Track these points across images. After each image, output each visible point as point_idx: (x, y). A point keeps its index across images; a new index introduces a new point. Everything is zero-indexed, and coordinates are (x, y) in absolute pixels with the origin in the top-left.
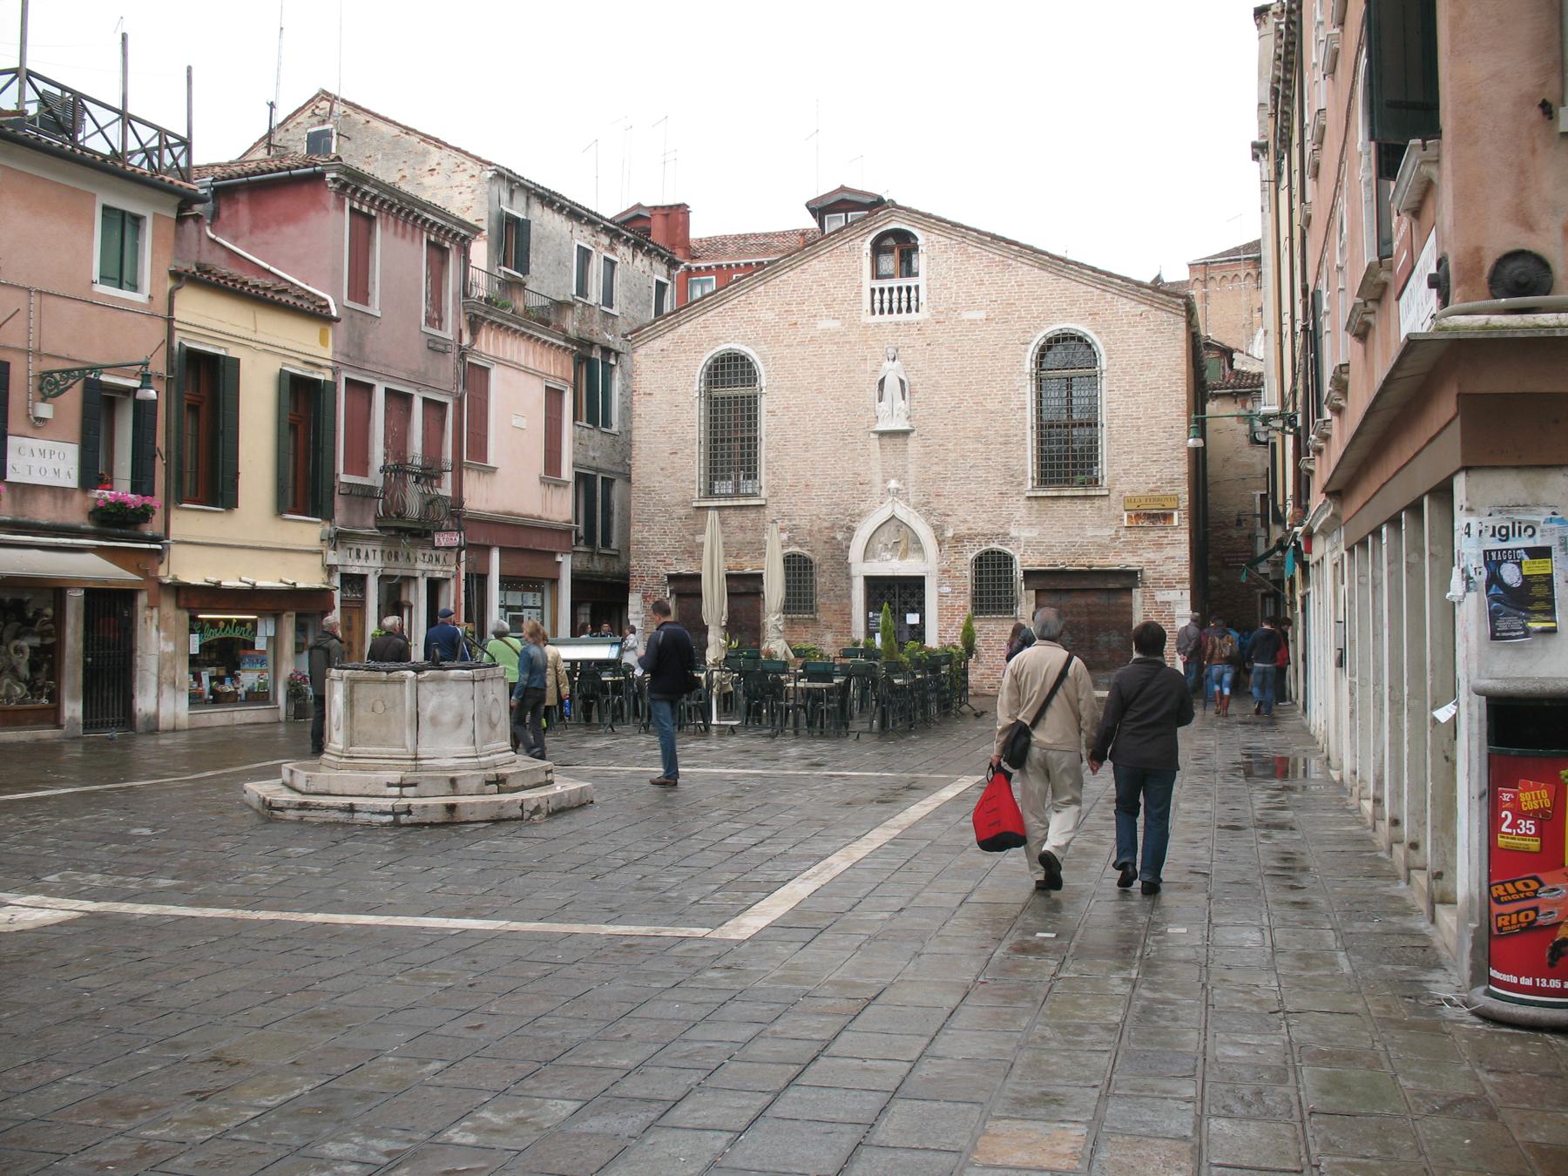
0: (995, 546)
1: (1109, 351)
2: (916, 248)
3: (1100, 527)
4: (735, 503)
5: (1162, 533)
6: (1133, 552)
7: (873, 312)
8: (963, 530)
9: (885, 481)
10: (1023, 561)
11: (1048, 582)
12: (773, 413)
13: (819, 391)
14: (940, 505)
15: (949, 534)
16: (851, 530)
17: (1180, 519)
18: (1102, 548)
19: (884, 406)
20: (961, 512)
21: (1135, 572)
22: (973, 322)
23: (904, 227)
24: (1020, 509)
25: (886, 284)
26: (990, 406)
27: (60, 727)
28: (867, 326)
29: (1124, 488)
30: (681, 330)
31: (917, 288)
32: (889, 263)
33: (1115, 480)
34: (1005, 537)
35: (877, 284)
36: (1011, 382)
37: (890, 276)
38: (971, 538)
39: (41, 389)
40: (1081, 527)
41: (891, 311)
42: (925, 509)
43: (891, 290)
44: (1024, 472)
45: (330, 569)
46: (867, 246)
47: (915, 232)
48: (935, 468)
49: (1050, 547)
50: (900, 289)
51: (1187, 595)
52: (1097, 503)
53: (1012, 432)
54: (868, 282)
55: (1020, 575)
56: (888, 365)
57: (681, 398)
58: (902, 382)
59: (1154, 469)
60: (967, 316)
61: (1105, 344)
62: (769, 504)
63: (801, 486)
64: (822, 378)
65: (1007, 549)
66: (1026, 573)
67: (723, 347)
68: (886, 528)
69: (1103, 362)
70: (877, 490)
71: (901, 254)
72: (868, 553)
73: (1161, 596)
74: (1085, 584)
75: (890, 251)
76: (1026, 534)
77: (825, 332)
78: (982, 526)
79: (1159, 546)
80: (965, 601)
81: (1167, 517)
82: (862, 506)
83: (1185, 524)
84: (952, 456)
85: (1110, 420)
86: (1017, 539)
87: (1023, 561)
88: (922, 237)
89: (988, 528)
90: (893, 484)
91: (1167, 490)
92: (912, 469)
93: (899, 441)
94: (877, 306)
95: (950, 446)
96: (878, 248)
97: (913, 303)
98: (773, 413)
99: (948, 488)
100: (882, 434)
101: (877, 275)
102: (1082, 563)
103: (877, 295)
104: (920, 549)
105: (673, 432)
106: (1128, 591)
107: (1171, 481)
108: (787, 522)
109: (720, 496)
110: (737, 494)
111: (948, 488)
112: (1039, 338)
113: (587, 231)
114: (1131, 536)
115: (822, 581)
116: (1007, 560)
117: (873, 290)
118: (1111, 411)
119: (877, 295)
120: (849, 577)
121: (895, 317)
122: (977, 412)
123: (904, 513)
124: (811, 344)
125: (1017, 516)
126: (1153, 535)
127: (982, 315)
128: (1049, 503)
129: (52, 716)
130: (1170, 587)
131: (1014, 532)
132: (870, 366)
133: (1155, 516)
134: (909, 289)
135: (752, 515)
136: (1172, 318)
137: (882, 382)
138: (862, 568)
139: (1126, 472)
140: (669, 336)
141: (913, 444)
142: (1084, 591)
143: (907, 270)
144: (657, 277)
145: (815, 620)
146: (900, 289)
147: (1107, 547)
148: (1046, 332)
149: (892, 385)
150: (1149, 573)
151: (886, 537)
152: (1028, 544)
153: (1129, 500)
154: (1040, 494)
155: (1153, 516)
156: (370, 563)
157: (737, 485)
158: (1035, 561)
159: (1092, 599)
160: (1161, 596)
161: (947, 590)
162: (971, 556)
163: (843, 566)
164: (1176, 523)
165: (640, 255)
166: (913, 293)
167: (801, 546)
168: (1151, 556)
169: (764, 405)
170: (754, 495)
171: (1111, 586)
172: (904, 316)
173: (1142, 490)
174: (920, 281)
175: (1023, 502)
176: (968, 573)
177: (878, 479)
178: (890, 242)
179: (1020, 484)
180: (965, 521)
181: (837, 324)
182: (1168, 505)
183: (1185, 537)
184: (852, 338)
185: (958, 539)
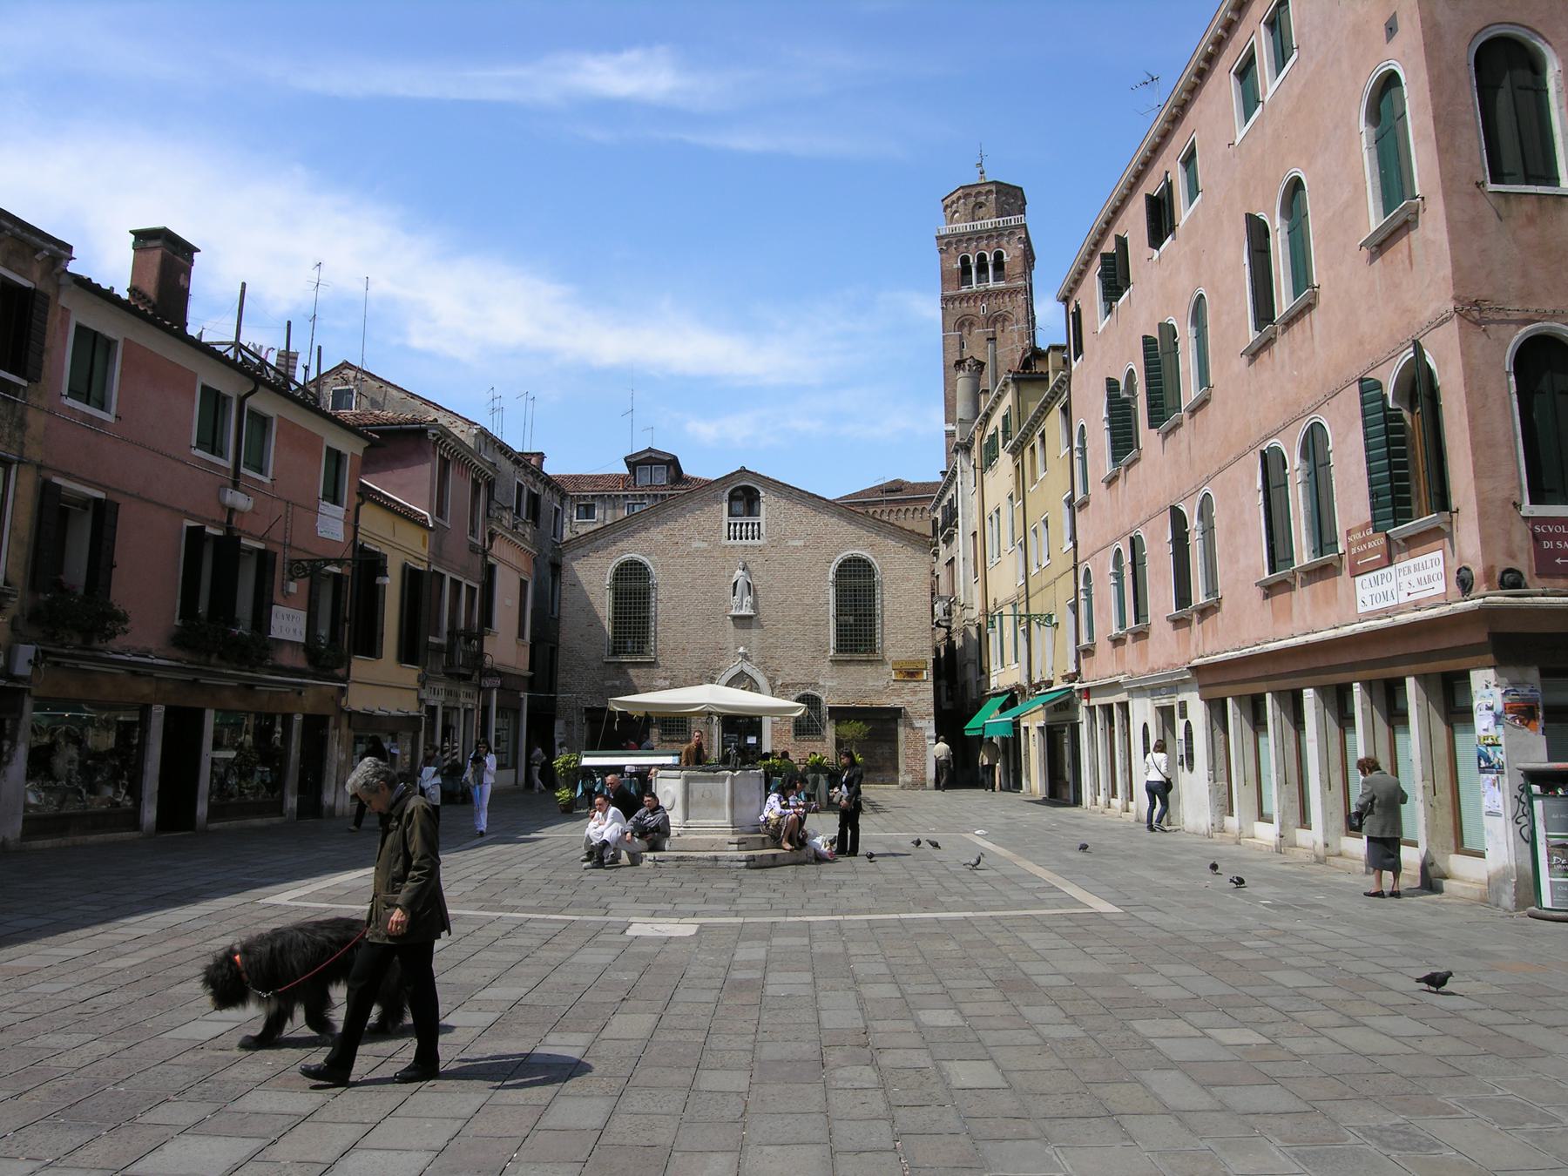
0: (809, 691)
8: (788, 680)
10: (828, 700)
14: (774, 664)
17: (927, 675)
22: (796, 547)
24: (826, 667)
25: (738, 520)
27: (282, 815)
34: (816, 685)
38: (794, 685)
39: (290, 571)
42: (763, 666)
45: (421, 701)
46: (726, 496)
51: (933, 723)
67: (627, 557)
75: (739, 499)
78: (800, 678)
83: (931, 678)
87: (828, 700)
88: (762, 494)
89: (805, 679)
90: (741, 650)
91: (920, 657)
111: (779, 652)
112: (838, 559)
114: (897, 685)
123: (748, 668)
124: (687, 561)
126: (911, 685)
127: (801, 543)
129: (278, 808)
152: (831, 689)
153: (895, 663)
155: (912, 674)
156: (437, 701)
173: (904, 657)
174: (762, 519)
177: (732, 646)
178: (740, 493)
181: (705, 545)
183: (930, 686)
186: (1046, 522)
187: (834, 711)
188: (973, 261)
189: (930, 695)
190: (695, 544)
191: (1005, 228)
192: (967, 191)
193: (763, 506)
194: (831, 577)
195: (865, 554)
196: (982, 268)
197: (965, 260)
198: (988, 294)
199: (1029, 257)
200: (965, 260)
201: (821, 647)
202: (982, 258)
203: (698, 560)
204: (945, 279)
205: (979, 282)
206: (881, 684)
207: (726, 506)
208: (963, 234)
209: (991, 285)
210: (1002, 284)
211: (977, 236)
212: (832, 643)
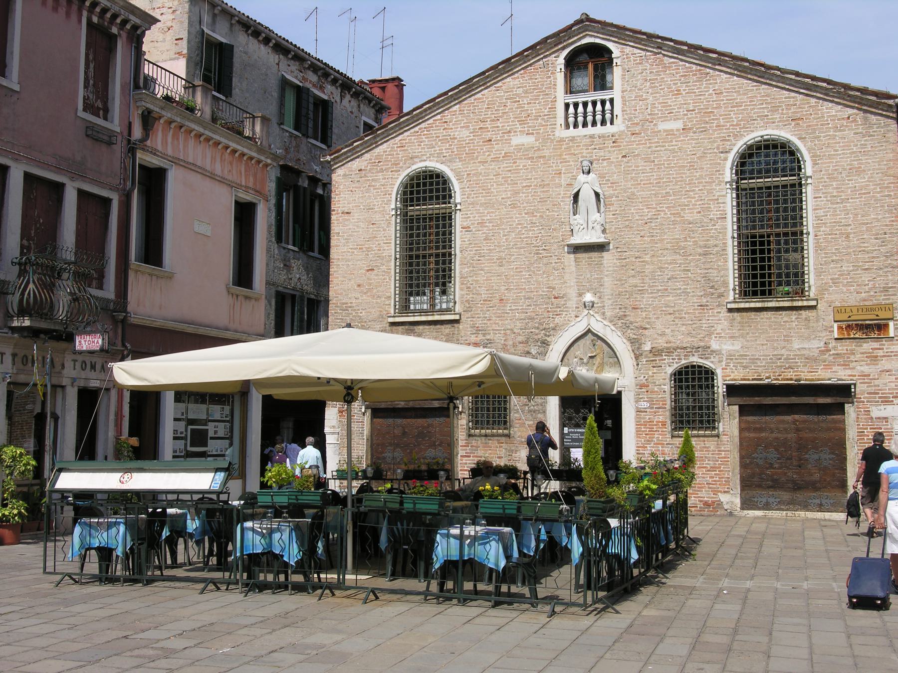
0: (695, 360)
1: (814, 157)
2: (611, 60)
3: (808, 339)
4: (430, 318)
5: (876, 345)
6: (845, 365)
7: (567, 126)
8: (661, 343)
9: (580, 295)
11: (754, 398)
12: (466, 228)
13: (514, 206)
15: (647, 347)
16: (545, 344)
19: (579, 219)
20: (659, 325)
21: (848, 387)
22: (669, 132)
23: (598, 41)
24: (722, 321)
25: (580, 98)
26: (688, 217)
28: (562, 140)
29: (833, 297)
30: (377, 150)
31: (612, 101)
32: (584, 80)
33: (822, 290)
34: (705, 350)
35: (571, 99)
36: (710, 192)
38: (669, 351)
40: (788, 339)
41: (585, 125)
42: (622, 321)
43: (585, 104)
44: (725, 284)
47: (610, 45)
48: (633, 281)
49: (754, 360)
50: (594, 103)
52: (804, 314)
53: (711, 242)
54: (561, 97)
55: (720, 389)
56: (582, 178)
57: (377, 217)
58: (597, 195)
59: (866, 278)
60: (663, 126)
61: (809, 150)
62: (463, 319)
63: (496, 301)
64: (516, 193)
65: (708, 363)
67: (419, 166)
69: (808, 169)
70: (572, 303)
71: (596, 69)
76: (727, 347)
77: (519, 148)
78: (681, 339)
80: (665, 416)
84: (649, 268)
85: (817, 227)
89: (687, 341)
90: (588, 297)
91: (882, 299)
92: (608, 282)
94: (571, 120)
95: (647, 258)
96: (573, 64)
97: (608, 116)
98: (466, 228)
99: (645, 300)
100: (578, 249)
101: (570, 90)
102: (788, 377)
103: (571, 109)
104: (618, 363)
105: (369, 249)
106: (840, 409)
108: (481, 337)
109: (415, 312)
110: (432, 310)
111: (645, 300)
112: (739, 146)
113: (295, 66)
114: (842, 348)
116: (708, 375)
117: (567, 106)
118: (818, 218)
119: (571, 109)
121: (590, 130)
122: (674, 223)
123: (598, 327)
125: (719, 328)
126: (868, 346)
127: (678, 125)
128: (752, 315)
131: (715, 346)
133: (868, 327)
134: (603, 103)
136: (882, 120)
137: (576, 196)
139: (835, 282)
140: (367, 156)
142: (791, 409)
143: (601, 83)
144: (364, 118)
145: (508, 436)
147: (815, 360)
148: (745, 139)
149: (587, 196)
150: (861, 389)
152: (730, 356)
153: (838, 310)
154: (742, 305)
158: (739, 376)
161: (644, 405)
162: (670, 370)
164: (892, 334)
165: (348, 97)
168: (866, 369)
169: (459, 220)
170: (448, 310)
172: (599, 129)
173: (853, 300)
174: (616, 93)
175: (724, 314)
176: (667, 388)
177: (573, 293)
178: (584, 57)
179: (721, 295)
180: (663, 334)
181: (531, 139)
184: (546, 153)
187: (733, 390)
190: (518, 140)
194: (728, 174)
201: (713, 289)
203: (521, 163)
206: (816, 345)
207: (560, 78)
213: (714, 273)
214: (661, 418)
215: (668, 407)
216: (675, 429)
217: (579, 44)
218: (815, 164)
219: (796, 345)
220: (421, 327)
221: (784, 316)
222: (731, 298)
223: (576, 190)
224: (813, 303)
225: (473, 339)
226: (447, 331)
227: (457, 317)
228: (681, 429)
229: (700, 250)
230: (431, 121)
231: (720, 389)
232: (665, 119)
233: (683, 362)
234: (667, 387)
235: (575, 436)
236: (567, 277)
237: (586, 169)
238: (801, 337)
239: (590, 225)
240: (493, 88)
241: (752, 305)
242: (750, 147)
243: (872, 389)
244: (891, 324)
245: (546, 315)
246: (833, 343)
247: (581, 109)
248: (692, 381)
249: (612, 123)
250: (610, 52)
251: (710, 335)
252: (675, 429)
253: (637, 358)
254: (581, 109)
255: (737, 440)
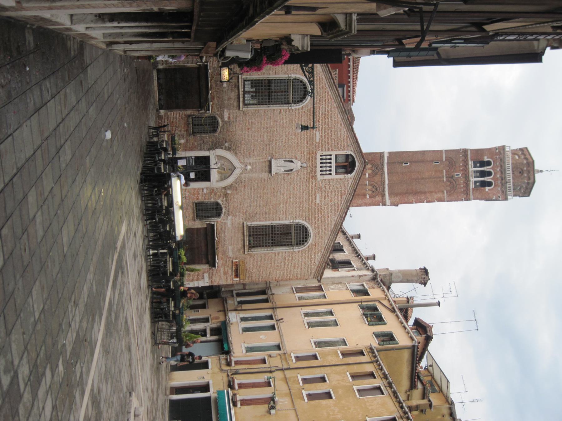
0: (224, 210)
3: (232, 251)
5: (230, 274)
7: (321, 156)
9: (250, 164)
15: (229, 192)
16: (229, 149)
18: (225, 253)
21: (214, 266)
24: (239, 219)
25: (333, 161)
28: (316, 154)
31: (331, 174)
32: (341, 160)
34: (227, 214)
35: (333, 157)
37: (336, 162)
38: (227, 200)
43: (330, 163)
44: (254, 221)
46: (349, 152)
47: (354, 173)
49: (224, 232)
51: (207, 285)
52: (242, 250)
54: (334, 153)
56: (299, 163)
58: (292, 170)
62: (240, 112)
63: (249, 127)
65: (222, 215)
66: (213, 226)
68: (230, 164)
69: (297, 249)
70: (247, 160)
72: (220, 157)
73: (206, 276)
74: (210, 247)
79: (225, 274)
80: (201, 199)
81: (237, 276)
82: (240, 154)
86: (227, 219)
89: (231, 206)
90: (249, 167)
92: (255, 175)
93: (267, 169)
94: (324, 157)
96: (347, 156)
97: (324, 173)
106: (207, 263)
107: (250, 277)
109: (244, 85)
114: (229, 263)
115: (207, 137)
116: (219, 215)
117: (331, 155)
119: (329, 157)
120: (209, 149)
121: (319, 165)
123: (237, 172)
126: (230, 272)
128: (242, 231)
130: (210, 278)
131: (229, 218)
132: (298, 156)
134: (330, 171)
135: (235, 104)
137: (292, 162)
138: (213, 155)
141: (265, 175)
142: (207, 245)
146: (330, 167)
149: (290, 166)
151: (226, 165)
157: (249, 92)
159: (203, 248)
160: (206, 276)
161: (205, 191)
162: (219, 201)
163: (213, 147)
164: (234, 279)
166: (328, 172)
167: (222, 127)
168: (222, 271)
171: (209, 256)
172: (319, 169)
174: (334, 176)
175: (242, 221)
177: (251, 160)
178: (350, 160)
181: (318, 140)
182: (241, 276)
183: (230, 282)
185: (226, 195)
186: (328, 395)
187: (212, 227)
188: (486, 169)
189: (223, 282)
191: (506, 188)
192: (531, 164)
193: (342, 176)
195: (311, 241)
196: (483, 174)
197: (489, 163)
198: (466, 177)
199: (488, 199)
200: (489, 163)
201: (252, 216)
202: (489, 174)
204: (478, 152)
205: (474, 172)
208: (504, 163)
209: (472, 180)
210: (472, 186)
211: (503, 171)
212: (255, 223)
213: (258, 216)
214: (200, 198)
215: (205, 201)
216: (196, 204)
217: (356, 160)
218: (298, 252)
219: (230, 247)
220: (237, 91)
221: (241, 242)
222: (248, 223)
223: (293, 160)
224: (246, 253)
225: (232, 116)
226: (235, 104)
227: (241, 109)
228: (196, 206)
229: (267, 211)
230: (330, 93)
231: (213, 221)
232: (321, 196)
233: (223, 206)
234: (212, 200)
235: (191, 161)
236: (258, 158)
237: (303, 165)
238: (233, 249)
239: (279, 168)
240: (342, 122)
241: (245, 232)
242: (306, 229)
243: (214, 273)
244: (238, 279)
245: (242, 149)
246: (231, 260)
247: (329, 161)
248: (215, 210)
249: (321, 175)
250: (350, 172)
251: (234, 216)
252: (196, 204)
253: (224, 188)
254: (329, 161)
255: (193, 227)
